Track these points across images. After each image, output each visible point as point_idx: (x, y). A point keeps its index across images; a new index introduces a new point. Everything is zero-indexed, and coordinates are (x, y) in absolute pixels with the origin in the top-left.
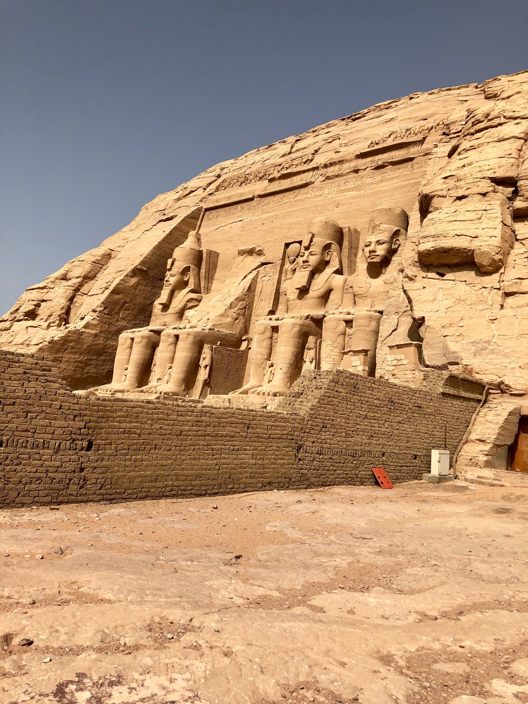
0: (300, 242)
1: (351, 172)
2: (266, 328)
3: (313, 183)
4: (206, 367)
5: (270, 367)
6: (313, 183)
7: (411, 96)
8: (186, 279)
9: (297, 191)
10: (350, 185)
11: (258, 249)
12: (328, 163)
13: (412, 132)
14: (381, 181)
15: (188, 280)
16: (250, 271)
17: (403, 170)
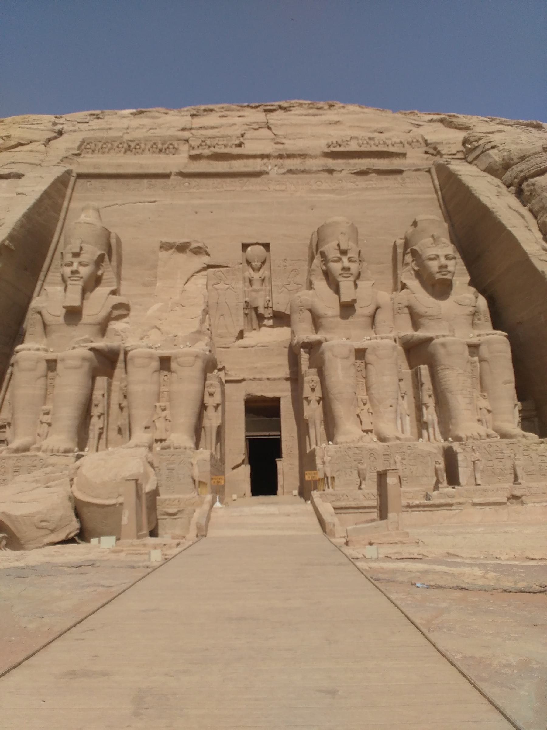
0: (267, 246)
1: (323, 170)
2: (350, 351)
3: (267, 173)
4: (216, 407)
5: (365, 404)
6: (267, 173)
7: (331, 103)
8: (100, 273)
9: (245, 179)
10: (324, 186)
12: (284, 153)
13: (382, 142)
14: (366, 189)
15: (102, 274)
17: (390, 181)
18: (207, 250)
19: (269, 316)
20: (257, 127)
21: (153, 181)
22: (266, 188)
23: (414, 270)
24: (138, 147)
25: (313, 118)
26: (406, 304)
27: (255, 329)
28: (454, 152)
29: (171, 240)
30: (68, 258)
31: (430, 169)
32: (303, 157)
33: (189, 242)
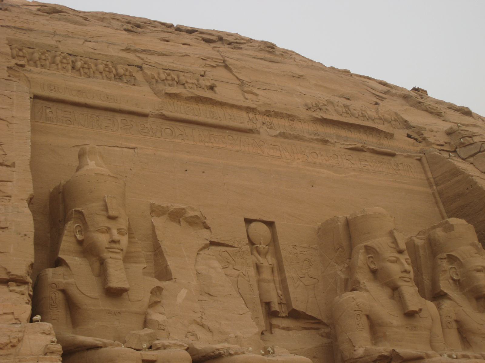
0: (270, 224)
1: (316, 140)
3: (258, 133)
11: (190, 213)
13: (360, 114)
18: (205, 220)
19: (284, 315)
20: (214, 64)
22: (260, 152)
23: (453, 279)
24: (86, 66)
25: (270, 64)
26: (454, 317)
28: (442, 142)
30: (104, 223)
31: (421, 157)
32: (290, 118)
33: (184, 209)
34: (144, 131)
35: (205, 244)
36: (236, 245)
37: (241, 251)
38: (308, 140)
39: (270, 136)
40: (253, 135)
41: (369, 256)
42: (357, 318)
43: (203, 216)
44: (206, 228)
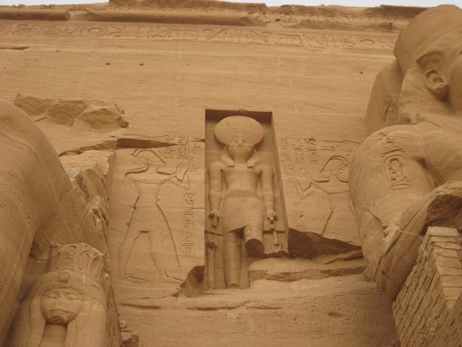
0: (265, 118)
9: (217, 28)
11: (96, 108)
16: (77, 147)
18: (122, 115)
19: (277, 250)
21: (30, 23)
22: (259, 41)
27: (235, 286)
29: (42, 95)
32: (328, 14)
33: (81, 102)
34: (53, 32)
35: (107, 141)
36: (175, 141)
37: (182, 149)
38: (357, 28)
39: (284, 27)
40: (252, 27)
41: (428, 71)
42: (391, 168)
43: (119, 110)
44: (122, 127)
